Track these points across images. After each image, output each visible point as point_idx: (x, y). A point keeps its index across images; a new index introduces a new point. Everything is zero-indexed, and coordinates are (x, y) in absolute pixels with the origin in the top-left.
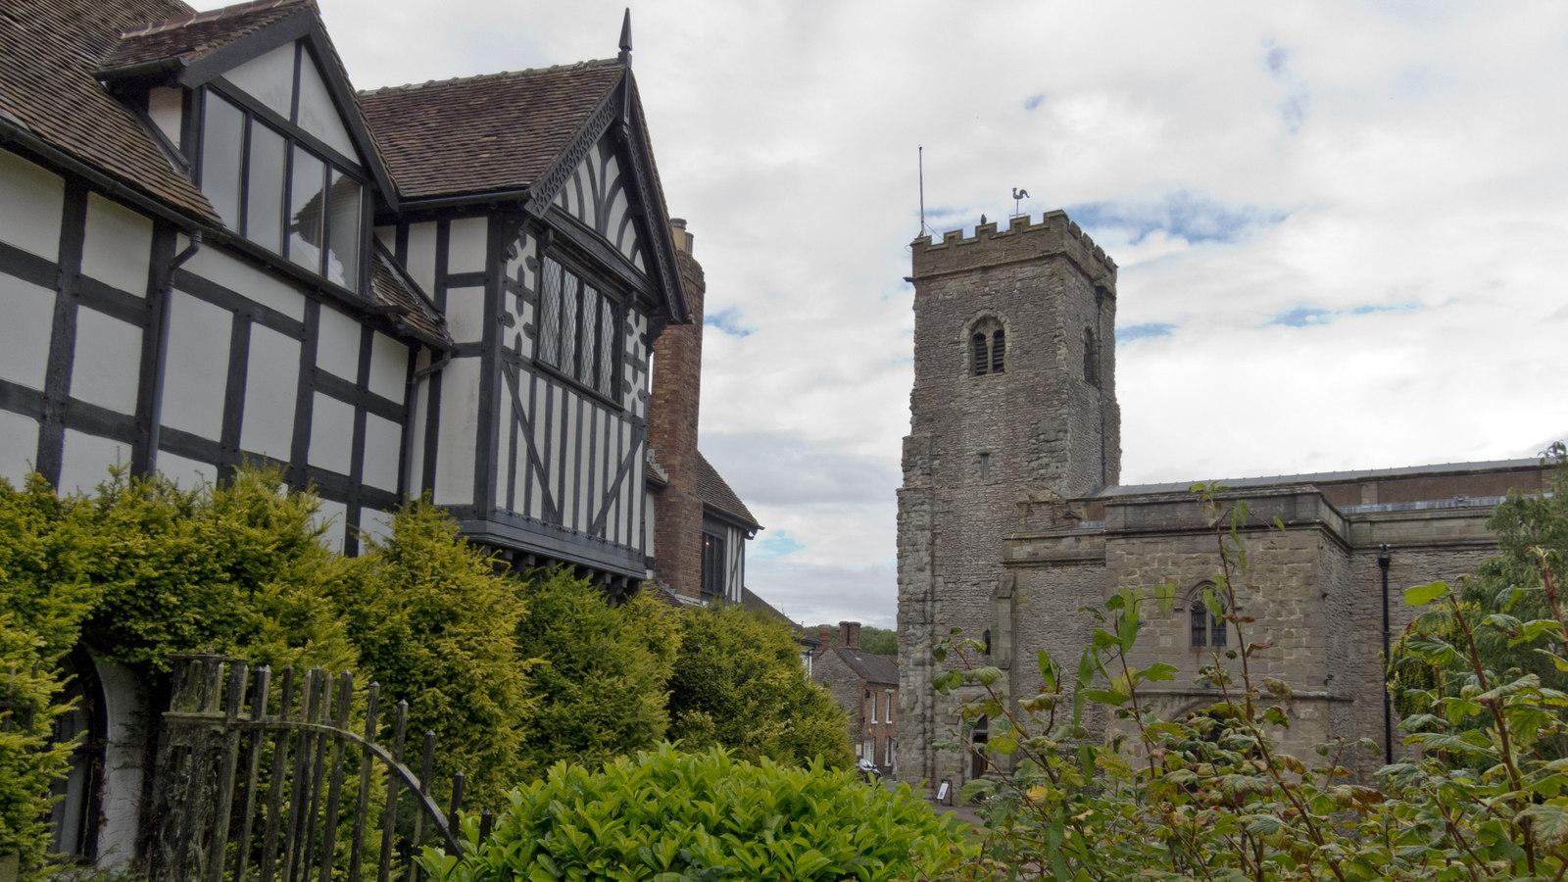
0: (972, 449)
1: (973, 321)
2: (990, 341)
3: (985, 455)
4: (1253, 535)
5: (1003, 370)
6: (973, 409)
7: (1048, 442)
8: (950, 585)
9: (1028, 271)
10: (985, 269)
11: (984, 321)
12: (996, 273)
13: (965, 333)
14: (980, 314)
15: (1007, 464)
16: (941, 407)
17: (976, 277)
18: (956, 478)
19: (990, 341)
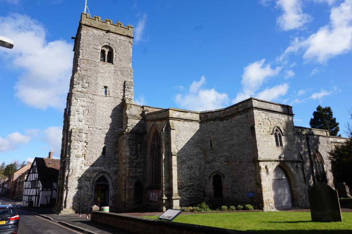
0: (102, 83)
1: (103, 45)
2: (107, 53)
3: (106, 87)
4: (283, 115)
5: (113, 64)
6: (102, 71)
7: (128, 88)
8: (90, 129)
9: (122, 38)
10: (108, 31)
11: (106, 46)
12: (111, 34)
13: (100, 48)
14: (106, 44)
15: (113, 92)
16: (90, 67)
17: (104, 32)
18: (95, 92)
19: (107, 53)
